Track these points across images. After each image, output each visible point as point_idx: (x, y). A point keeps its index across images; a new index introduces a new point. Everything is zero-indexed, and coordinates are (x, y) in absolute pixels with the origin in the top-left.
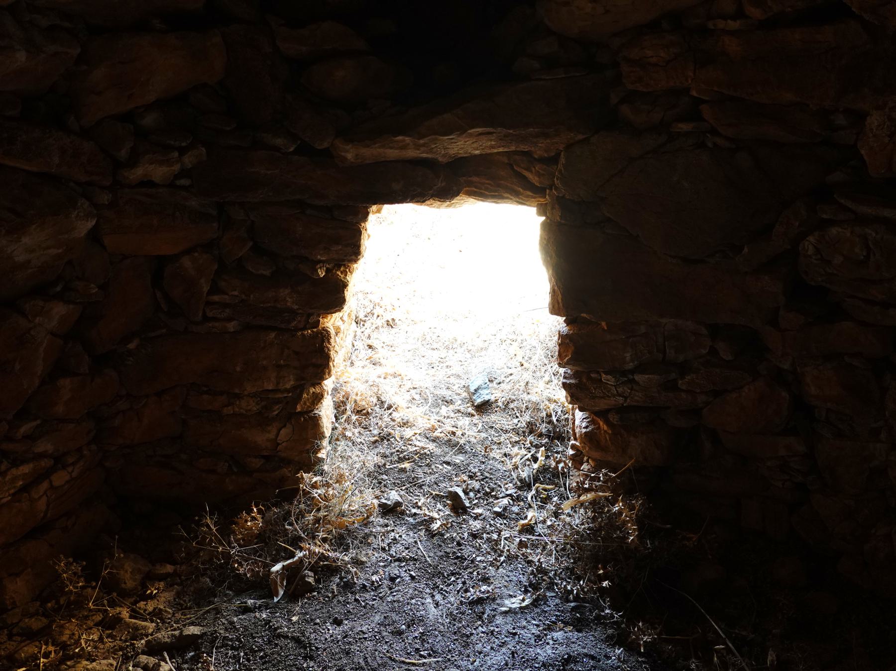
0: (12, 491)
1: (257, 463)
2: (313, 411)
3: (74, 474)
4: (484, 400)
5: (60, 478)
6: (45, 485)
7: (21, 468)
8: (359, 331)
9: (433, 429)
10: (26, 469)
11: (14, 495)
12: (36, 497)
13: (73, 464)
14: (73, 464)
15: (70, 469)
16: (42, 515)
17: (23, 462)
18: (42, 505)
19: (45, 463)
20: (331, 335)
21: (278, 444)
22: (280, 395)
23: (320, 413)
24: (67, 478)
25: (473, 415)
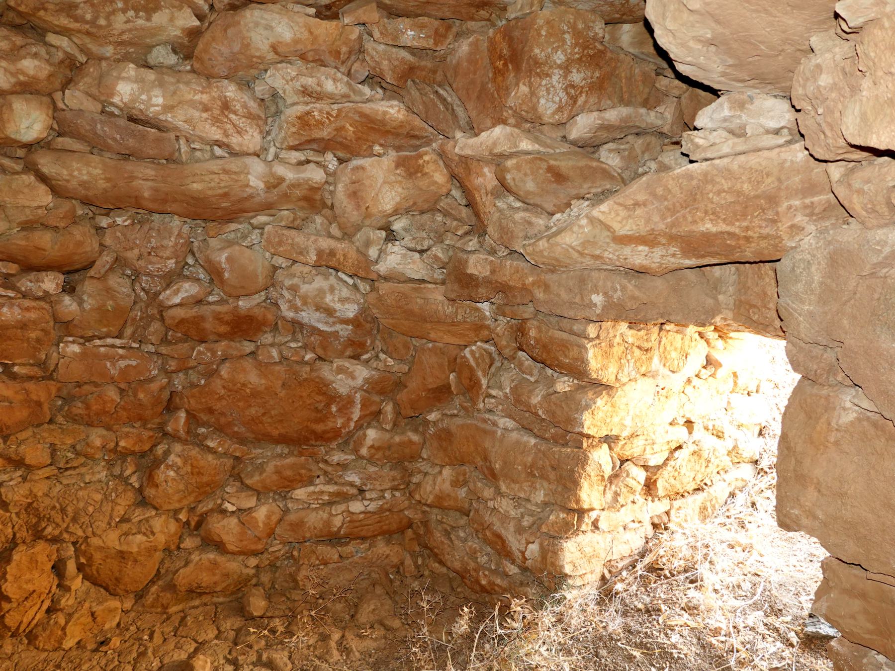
0: (320, 502)
1: (513, 570)
2: (561, 538)
3: (370, 508)
4: (817, 632)
5: (356, 507)
6: (341, 508)
7: (328, 486)
8: (753, 481)
9: (716, 632)
10: (331, 488)
11: (323, 504)
12: (334, 513)
13: (371, 500)
14: (371, 500)
15: (366, 503)
16: (336, 529)
17: (336, 483)
18: (337, 522)
19: (354, 491)
20: (589, 462)
21: (527, 559)
22: (529, 506)
23: (565, 545)
24: (363, 509)
25: (792, 645)
